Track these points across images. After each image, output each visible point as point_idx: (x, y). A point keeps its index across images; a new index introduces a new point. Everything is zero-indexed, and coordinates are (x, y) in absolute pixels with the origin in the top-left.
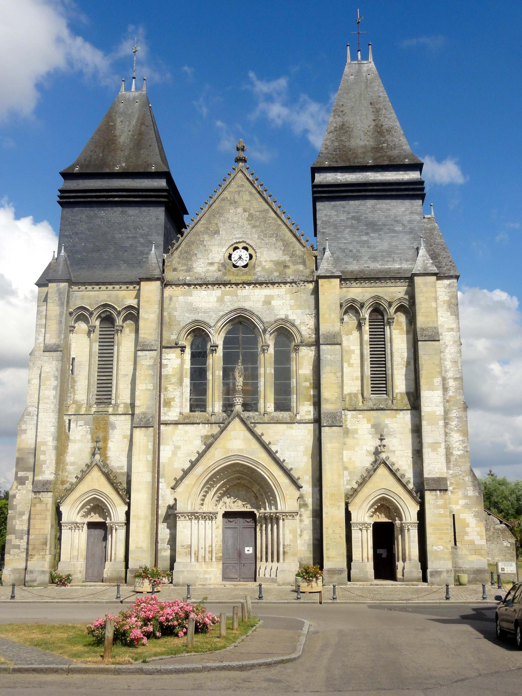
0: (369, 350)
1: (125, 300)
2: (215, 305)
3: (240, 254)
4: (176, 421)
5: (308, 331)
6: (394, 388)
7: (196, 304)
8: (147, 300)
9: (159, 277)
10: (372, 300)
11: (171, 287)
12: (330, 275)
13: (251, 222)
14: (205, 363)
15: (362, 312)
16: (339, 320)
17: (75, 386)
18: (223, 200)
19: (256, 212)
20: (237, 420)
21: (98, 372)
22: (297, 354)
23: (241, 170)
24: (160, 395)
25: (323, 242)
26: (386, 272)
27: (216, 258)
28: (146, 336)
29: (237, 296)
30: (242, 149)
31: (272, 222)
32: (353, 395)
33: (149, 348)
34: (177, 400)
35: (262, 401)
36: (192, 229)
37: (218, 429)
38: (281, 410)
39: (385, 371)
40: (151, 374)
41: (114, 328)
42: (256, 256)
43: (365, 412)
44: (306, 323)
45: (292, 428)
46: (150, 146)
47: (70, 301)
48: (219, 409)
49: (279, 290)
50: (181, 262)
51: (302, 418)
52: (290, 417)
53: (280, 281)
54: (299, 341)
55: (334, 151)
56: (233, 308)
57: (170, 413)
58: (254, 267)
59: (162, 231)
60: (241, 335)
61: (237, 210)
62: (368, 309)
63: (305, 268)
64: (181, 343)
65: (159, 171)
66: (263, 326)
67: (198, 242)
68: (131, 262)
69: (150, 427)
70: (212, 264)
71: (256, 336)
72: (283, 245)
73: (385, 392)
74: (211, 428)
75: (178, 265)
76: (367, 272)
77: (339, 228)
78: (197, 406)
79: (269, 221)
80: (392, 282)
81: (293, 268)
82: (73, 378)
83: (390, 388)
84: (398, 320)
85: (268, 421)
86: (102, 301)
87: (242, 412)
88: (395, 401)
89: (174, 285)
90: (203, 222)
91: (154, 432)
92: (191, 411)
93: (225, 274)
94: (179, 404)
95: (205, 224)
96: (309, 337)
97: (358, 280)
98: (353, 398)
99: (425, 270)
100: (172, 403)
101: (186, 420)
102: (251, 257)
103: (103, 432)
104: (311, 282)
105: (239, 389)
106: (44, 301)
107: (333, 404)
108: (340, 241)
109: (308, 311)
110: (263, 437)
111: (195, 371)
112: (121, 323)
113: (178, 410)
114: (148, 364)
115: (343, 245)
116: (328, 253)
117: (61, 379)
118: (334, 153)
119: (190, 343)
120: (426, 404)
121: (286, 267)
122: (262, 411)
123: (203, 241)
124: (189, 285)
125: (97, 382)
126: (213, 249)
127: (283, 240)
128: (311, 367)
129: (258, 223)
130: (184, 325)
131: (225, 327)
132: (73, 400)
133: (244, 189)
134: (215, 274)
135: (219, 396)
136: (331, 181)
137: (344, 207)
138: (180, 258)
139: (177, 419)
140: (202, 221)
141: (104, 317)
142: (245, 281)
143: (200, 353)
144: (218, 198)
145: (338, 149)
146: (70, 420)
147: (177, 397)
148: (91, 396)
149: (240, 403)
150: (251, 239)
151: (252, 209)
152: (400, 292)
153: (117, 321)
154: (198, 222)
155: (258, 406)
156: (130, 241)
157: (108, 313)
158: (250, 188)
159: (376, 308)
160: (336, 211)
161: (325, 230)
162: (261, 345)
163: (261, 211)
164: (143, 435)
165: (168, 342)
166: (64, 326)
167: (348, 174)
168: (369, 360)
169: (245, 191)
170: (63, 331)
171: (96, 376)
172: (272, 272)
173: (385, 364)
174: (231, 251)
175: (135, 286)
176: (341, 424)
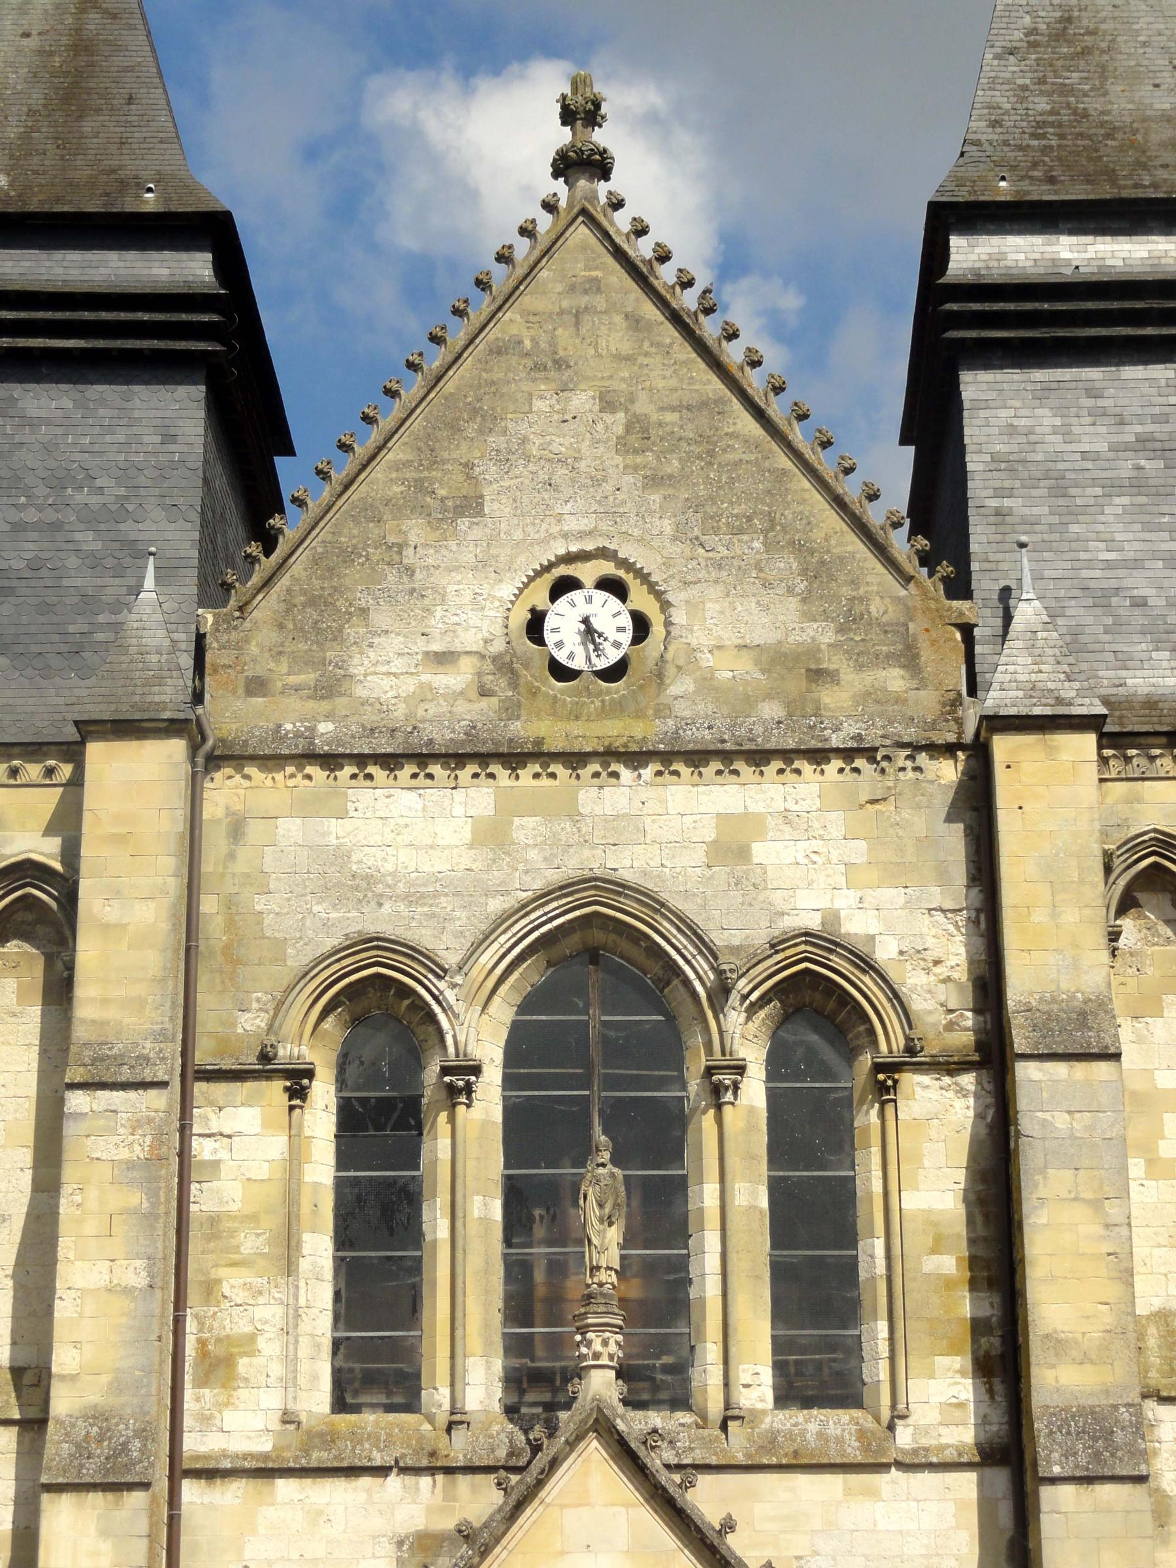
2: (466, 859)
3: (584, 609)
4: (265, 1456)
5: (942, 992)
7: (366, 860)
8: (115, 831)
9: (181, 716)
11: (239, 769)
12: (1048, 711)
13: (639, 460)
14: (411, 1156)
16: (1104, 941)
18: (498, 351)
19: (662, 409)
20: (593, 1450)
22: (889, 1108)
23: (584, 212)
24: (178, 1324)
25: (1000, 556)
27: (467, 629)
28: (111, 1014)
29: (575, 816)
30: (588, 112)
31: (745, 457)
33: (125, 1075)
34: (269, 1346)
35: (711, 1352)
36: (346, 487)
37: (496, 1498)
38: (807, 1403)
40: (135, 1211)
42: (668, 624)
44: (930, 956)
45: (873, 1493)
46: (130, 100)
48: (489, 1396)
49: (788, 788)
50: (290, 647)
51: (925, 1442)
52: (862, 1434)
53: (791, 744)
54: (898, 1042)
55: (1034, 136)
56: (554, 877)
57: (230, 1419)
58: (660, 676)
59: (191, 498)
60: (596, 1017)
61: (568, 400)
63: (914, 684)
64: (287, 1052)
65: (175, 207)
66: (712, 968)
67: (376, 554)
68: (34, 649)
69: (131, 1487)
70: (444, 659)
71: (671, 1018)
72: (804, 572)
74: (450, 1496)
75: (272, 665)
77: (1073, 491)
78: (370, 1380)
79: (731, 457)
81: (853, 681)
85: (748, 1456)
87: (621, 1409)
89: (253, 758)
90: (401, 456)
91: (151, 1516)
92: (340, 1404)
93: (511, 710)
94: (277, 1370)
95: (407, 464)
96: (950, 1026)
100: (243, 1365)
101: (315, 1454)
102: (641, 626)
104: (949, 750)
105: (601, 1285)
107: (1092, 1363)
108: (1083, 556)
109: (936, 896)
110: (731, 1540)
111: (359, 1198)
113: (272, 1400)
114: (124, 1154)
115: (1098, 573)
116: (1026, 612)
118: (1035, 143)
119: (333, 1057)
121: (818, 675)
122: (715, 1406)
123: (401, 547)
124: (330, 761)
126: (451, 588)
127: (799, 548)
128: (961, 1175)
129: (676, 463)
130: (306, 959)
131: (515, 975)
133: (600, 302)
134: (461, 707)
135: (486, 1325)
136: (1030, 271)
137: (1093, 393)
138: (281, 627)
139: (265, 1445)
140: (396, 453)
142: (618, 744)
143: (386, 1104)
144: (471, 342)
145: (1052, 124)
147: (271, 1331)
149: (611, 1357)
150: (640, 540)
151: (643, 396)
154: (372, 458)
155: (687, 1381)
156: (31, 546)
158: (633, 296)
160: (1059, 411)
161: (1007, 502)
162: (703, 1062)
163: (689, 408)
164: (92, 1529)
165: (224, 1045)
167: (1108, 239)
169: (606, 312)
172: (749, 701)
174: (539, 596)
175: (52, 763)
176: (1143, 1469)
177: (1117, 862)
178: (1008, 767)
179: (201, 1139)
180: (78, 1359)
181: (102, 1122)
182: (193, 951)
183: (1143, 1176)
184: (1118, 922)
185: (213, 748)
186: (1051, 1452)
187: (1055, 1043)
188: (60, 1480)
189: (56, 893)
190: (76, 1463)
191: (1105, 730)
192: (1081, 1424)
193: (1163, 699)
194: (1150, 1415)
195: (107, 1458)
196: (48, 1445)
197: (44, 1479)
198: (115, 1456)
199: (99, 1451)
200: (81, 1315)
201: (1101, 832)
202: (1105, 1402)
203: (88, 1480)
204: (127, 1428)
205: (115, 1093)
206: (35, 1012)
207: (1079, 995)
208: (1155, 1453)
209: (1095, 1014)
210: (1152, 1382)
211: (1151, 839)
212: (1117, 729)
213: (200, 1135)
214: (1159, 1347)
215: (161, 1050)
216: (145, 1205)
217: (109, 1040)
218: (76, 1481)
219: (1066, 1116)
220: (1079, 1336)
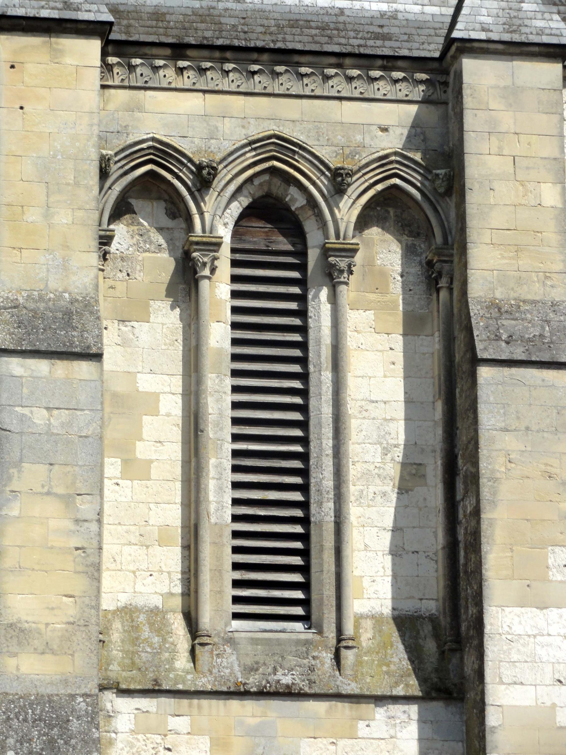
0: (229, 398)
6: (349, 590)
10: (250, 158)
12: (55, 15)
15: (201, 213)
16: (94, 244)
26: (323, 28)
32: (142, 618)
39: (304, 505)
43: (205, 703)
62: (234, 197)
73: (299, 611)
76: (233, 21)
80: (350, 79)
83: (329, 591)
84: (370, 263)
88: (348, 656)
97: (190, 53)
98: (146, 633)
99: (510, 28)
107: (53, 653)
120: (507, 673)
152: (385, 130)
159: (268, 195)
168: (229, 446)
173: (304, 473)
177: (114, 168)
178: (12, 67)
183: (119, 475)
184: (112, 227)
186: (7, 738)
187: (39, 340)
191: (110, 38)
192: (38, 712)
193: (171, 11)
194: (109, 706)
201: (100, 138)
202: (63, 691)
207: (67, 295)
208: (111, 742)
209: (81, 315)
210: (112, 675)
211: (149, 148)
212: (123, 37)
214: (123, 641)
219: (45, 412)
220: (42, 627)
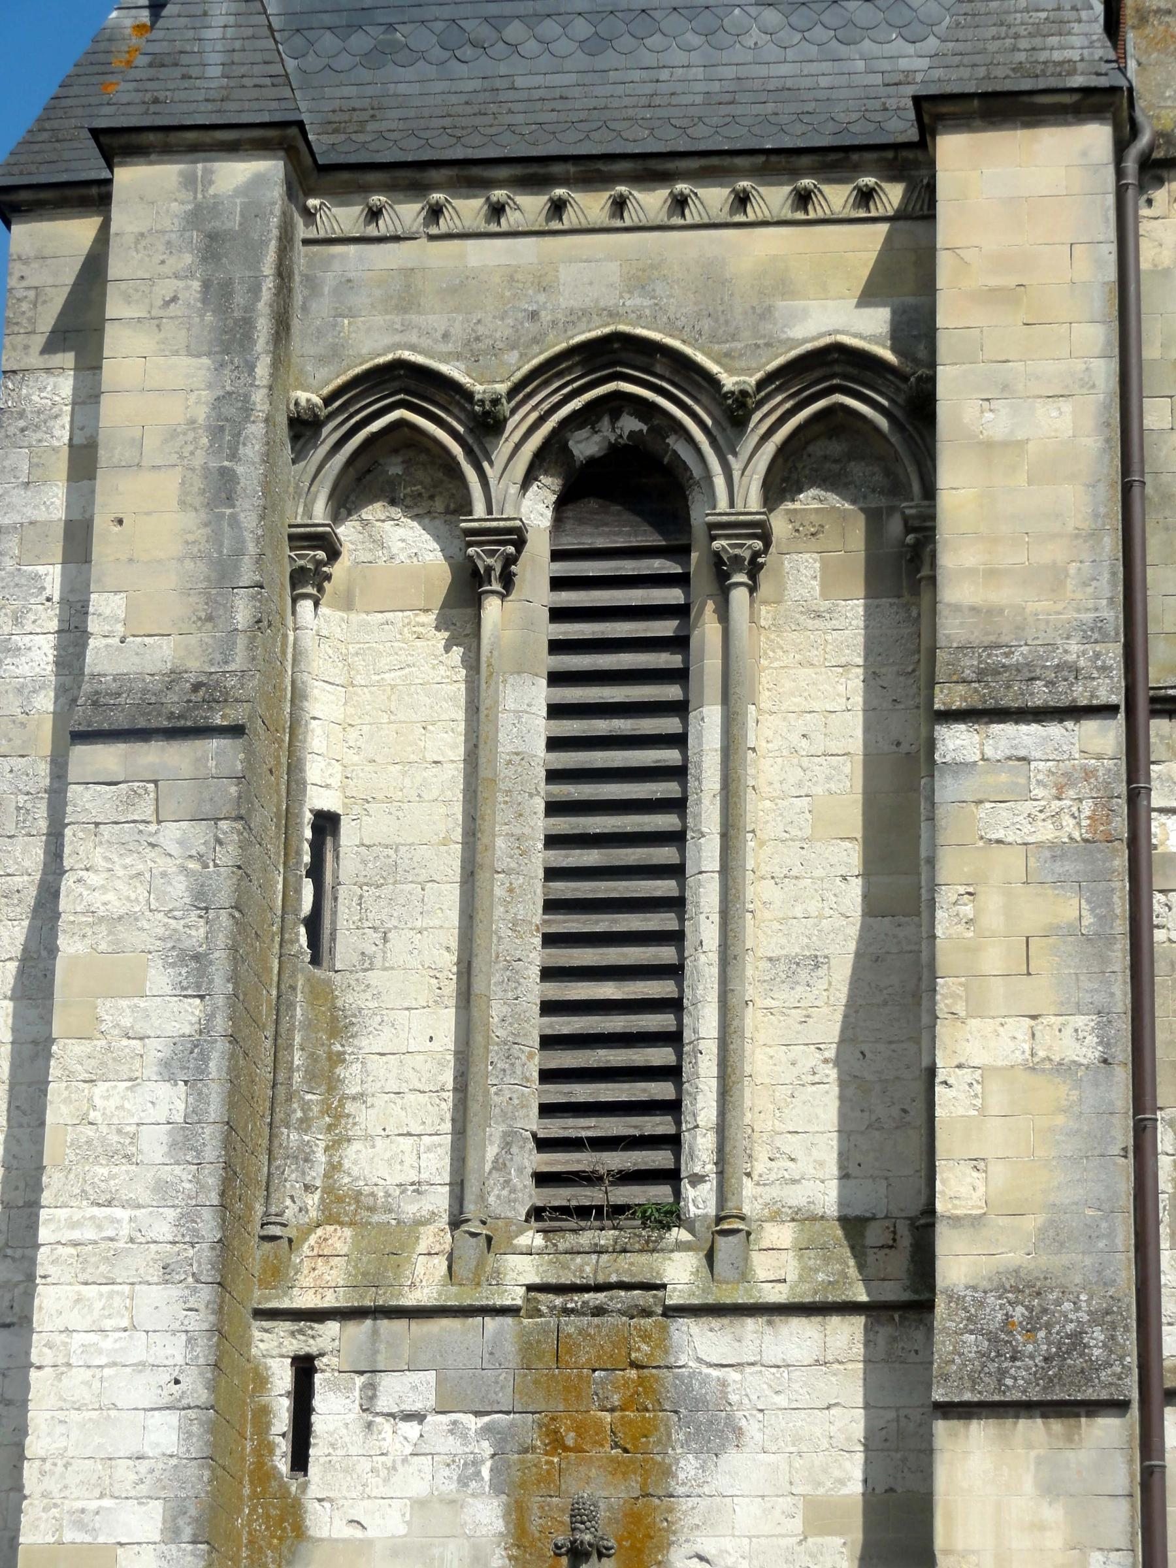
1: (781, 304)
8: (994, 281)
9: (1103, 82)
17: (338, 1059)
21: (550, 940)
28: (1003, 595)
33: (1040, 695)
40: (1072, 931)
41: (681, 552)
47: (296, 325)
69: (1093, 1408)
82: (322, 994)
86: (576, 316)
103: (618, 1469)
106: (58, 340)
112: (752, 499)
114: (1045, 832)
117: (234, 978)
125: (537, 1025)
132: (329, 1190)
141: (592, 461)
146: (304, 1368)
148: (492, 1151)
153: (719, 482)
157: (630, 424)
164: (1028, 1485)
166: (249, 520)
170: (247, 564)
171: (535, 972)
175: (870, 181)
179: (1163, 818)
180: (982, 1190)
181: (1004, 777)
182: (1136, 490)
185: (1152, 147)
188: (967, 1396)
189: (885, 403)
190: (992, 1367)
195: (1046, 1359)
196: (938, 1338)
197: (938, 1395)
198: (1062, 1355)
199: (1030, 1347)
200: (982, 1111)
203: (1016, 1396)
204: (1077, 1309)
205: (1023, 728)
206: (853, 610)
213: (1162, 811)
215: (1097, 656)
216: (1088, 919)
217: (1004, 639)
218: (996, 1398)
